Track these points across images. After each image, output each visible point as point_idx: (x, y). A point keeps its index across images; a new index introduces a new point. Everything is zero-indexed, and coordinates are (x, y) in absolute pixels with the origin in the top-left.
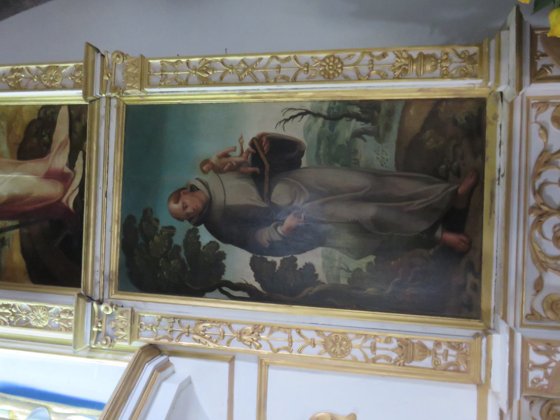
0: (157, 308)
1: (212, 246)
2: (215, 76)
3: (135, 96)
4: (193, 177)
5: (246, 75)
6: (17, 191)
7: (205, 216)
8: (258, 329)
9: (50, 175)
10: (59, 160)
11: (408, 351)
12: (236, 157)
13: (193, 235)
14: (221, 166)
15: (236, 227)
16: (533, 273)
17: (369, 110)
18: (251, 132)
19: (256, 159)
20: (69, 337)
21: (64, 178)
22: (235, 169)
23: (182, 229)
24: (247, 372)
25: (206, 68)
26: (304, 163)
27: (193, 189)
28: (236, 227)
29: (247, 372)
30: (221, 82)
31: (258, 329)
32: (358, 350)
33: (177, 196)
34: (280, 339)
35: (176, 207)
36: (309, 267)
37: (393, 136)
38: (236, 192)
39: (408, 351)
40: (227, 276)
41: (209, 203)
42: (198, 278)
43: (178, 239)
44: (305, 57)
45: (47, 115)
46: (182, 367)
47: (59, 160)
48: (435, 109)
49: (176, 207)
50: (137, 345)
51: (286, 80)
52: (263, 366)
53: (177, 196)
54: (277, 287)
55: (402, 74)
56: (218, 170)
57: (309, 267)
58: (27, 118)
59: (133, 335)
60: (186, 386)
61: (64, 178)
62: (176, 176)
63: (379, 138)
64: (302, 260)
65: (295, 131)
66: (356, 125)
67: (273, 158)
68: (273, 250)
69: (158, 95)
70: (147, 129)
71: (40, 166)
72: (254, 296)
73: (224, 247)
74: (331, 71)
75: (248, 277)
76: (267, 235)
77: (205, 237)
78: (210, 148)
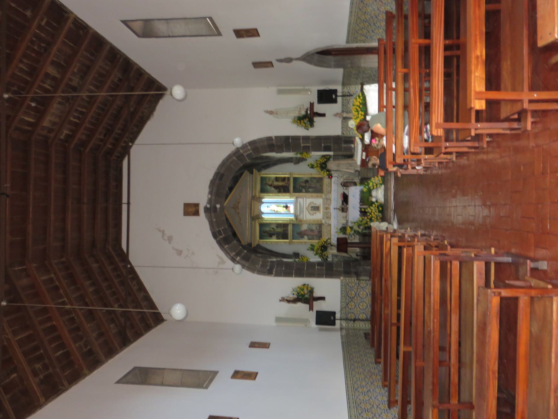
0: (297, 194)
5: (304, 175)
7: (301, 186)
10: (286, 181)
14: (302, 182)
17: (314, 178)
18: (305, 179)
24: (305, 199)
28: (304, 187)
38: (303, 184)
42: (300, 191)
45: (285, 178)
46: (299, 199)
47: (286, 181)
54: (307, 192)
65: (308, 179)
67: (307, 181)
69: (296, 176)
70: (295, 179)
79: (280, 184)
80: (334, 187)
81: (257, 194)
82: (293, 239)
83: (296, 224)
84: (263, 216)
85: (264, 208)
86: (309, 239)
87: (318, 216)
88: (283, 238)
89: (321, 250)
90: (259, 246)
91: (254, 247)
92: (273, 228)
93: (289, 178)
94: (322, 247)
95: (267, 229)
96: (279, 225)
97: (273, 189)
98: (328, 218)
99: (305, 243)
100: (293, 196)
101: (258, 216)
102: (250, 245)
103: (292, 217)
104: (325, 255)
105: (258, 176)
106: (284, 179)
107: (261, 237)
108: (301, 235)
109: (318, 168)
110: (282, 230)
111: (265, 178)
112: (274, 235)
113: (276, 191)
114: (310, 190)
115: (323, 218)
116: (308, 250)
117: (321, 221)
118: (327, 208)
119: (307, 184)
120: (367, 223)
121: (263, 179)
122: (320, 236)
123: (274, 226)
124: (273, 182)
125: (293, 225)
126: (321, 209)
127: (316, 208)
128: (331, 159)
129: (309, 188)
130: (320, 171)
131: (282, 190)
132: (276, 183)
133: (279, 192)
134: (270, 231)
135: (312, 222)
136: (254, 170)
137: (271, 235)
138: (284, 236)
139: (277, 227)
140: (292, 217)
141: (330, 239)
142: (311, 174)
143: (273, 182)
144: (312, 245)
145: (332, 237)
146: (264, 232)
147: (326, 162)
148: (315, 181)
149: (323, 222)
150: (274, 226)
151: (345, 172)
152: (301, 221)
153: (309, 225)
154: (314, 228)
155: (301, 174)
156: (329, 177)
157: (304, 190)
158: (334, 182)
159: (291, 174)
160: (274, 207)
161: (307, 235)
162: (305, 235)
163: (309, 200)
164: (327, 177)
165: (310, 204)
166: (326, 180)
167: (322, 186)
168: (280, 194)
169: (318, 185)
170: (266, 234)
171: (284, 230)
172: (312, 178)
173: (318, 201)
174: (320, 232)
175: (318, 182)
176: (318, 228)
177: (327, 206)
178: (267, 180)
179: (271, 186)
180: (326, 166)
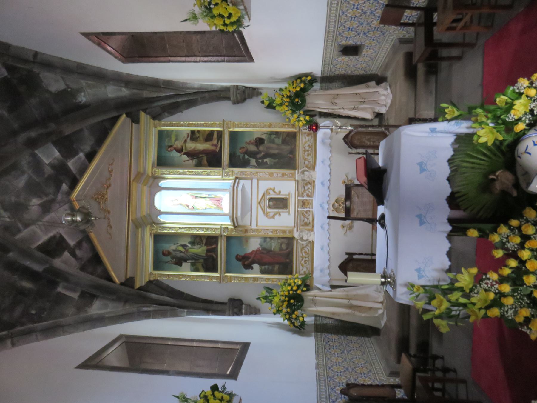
0: (236, 170)
1: (248, 158)
2: (248, 126)
3: (231, 130)
4: (244, 145)
5: (254, 126)
6: (205, 148)
8: (257, 173)
9: (213, 145)
10: (215, 142)
11: (283, 175)
12: (252, 141)
13: (244, 156)
14: (250, 143)
15: (253, 155)
16: (303, 161)
17: (277, 133)
18: (256, 136)
19: (256, 142)
20: (220, 177)
21: (216, 146)
22: (252, 144)
23: (242, 155)
24: (255, 181)
25: (247, 124)
26: (265, 142)
27: (244, 148)
28: (253, 155)
29: (255, 181)
30: (250, 127)
31: (257, 173)
32: (275, 175)
33: (241, 149)
34: (261, 174)
35: (240, 151)
36: (266, 162)
37: (281, 138)
38: (253, 148)
39: (283, 175)
40: (251, 164)
41: (247, 150)
42: (245, 164)
43: (241, 157)
44: (265, 124)
45: (211, 133)
46: (242, 182)
47: (215, 142)
48: (288, 134)
49: (240, 151)
50: (234, 177)
51: (262, 127)
52: (258, 180)
53: (241, 149)
54: (260, 165)
55: (282, 127)
56: (249, 144)
57: (266, 162)
58: (207, 133)
59: (233, 175)
60: (243, 185)
61: (216, 146)
62: (240, 145)
63: (279, 138)
64: (265, 160)
65: (264, 137)
66: (275, 136)
67: (260, 141)
68: (260, 159)
69: (236, 130)
70: (234, 136)
71: (210, 143)
72: (256, 167)
73: (250, 159)
74: (270, 126)
75: (255, 164)
76: (259, 156)
77: (246, 157)
78: (247, 140)
79: (201, 146)
80: (322, 152)
81: (149, 170)
82: (228, 271)
83: (235, 237)
84: (162, 218)
85: (163, 201)
86: (262, 272)
87: (285, 220)
88: (207, 270)
89: (289, 305)
90: (155, 285)
91: (141, 289)
92: (184, 246)
93: (220, 134)
94: (290, 297)
95: (171, 247)
96: (197, 239)
97: (185, 157)
98: (306, 224)
99: (255, 279)
100: (228, 175)
101: (151, 218)
102: (129, 282)
103: (227, 222)
104: (297, 318)
105: (149, 129)
106: (209, 136)
107: (158, 265)
108: (246, 261)
109: (285, 108)
110: (205, 251)
111: (168, 134)
112: (185, 260)
113: (194, 162)
114: (267, 160)
115: (296, 226)
116: (258, 299)
117: (291, 232)
118: (304, 204)
119: (261, 148)
120: (496, 303)
121: (161, 135)
122: (286, 267)
123: (186, 241)
124: (185, 142)
125: (228, 238)
126: (292, 203)
127: (280, 203)
128: (317, 86)
129: (267, 155)
130: (289, 113)
131: (205, 161)
132: (191, 146)
133: (199, 165)
134: (176, 250)
135: (271, 234)
136: (143, 116)
137: (179, 262)
138: (210, 264)
139: (193, 243)
140: (227, 222)
141: (312, 272)
142: (270, 126)
143: (185, 142)
144: (269, 289)
145: (316, 274)
146: (167, 254)
147: (303, 90)
148: (279, 141)
149: (296, 235)
150: (186, 241)
151: (348, 117)
152: (246, 231)
153: (265, 238)
154: (274, 246)
155: (246, 126)
156: (311, 128)
157: (253, 161)
158: (323, 142)
159: (224, 124)
160: (186, 198)
161: (261, 264)
162: (253, 262)
163: (264, 185)
164: (306, 130)
165: (267, 192)
166: (303, 141)
167: (293, 152)
168: (200, 171)
169: (286, 148)
170: (168, 258)
171: (208, 251)
172: (272, 133)
173: (285, 186)
174: (289, 255)
175: (284, 142)
176: (284, 247)
177: (306, 198)
178: (173, 139)
179: (180, 151)
180: (304, 101)
